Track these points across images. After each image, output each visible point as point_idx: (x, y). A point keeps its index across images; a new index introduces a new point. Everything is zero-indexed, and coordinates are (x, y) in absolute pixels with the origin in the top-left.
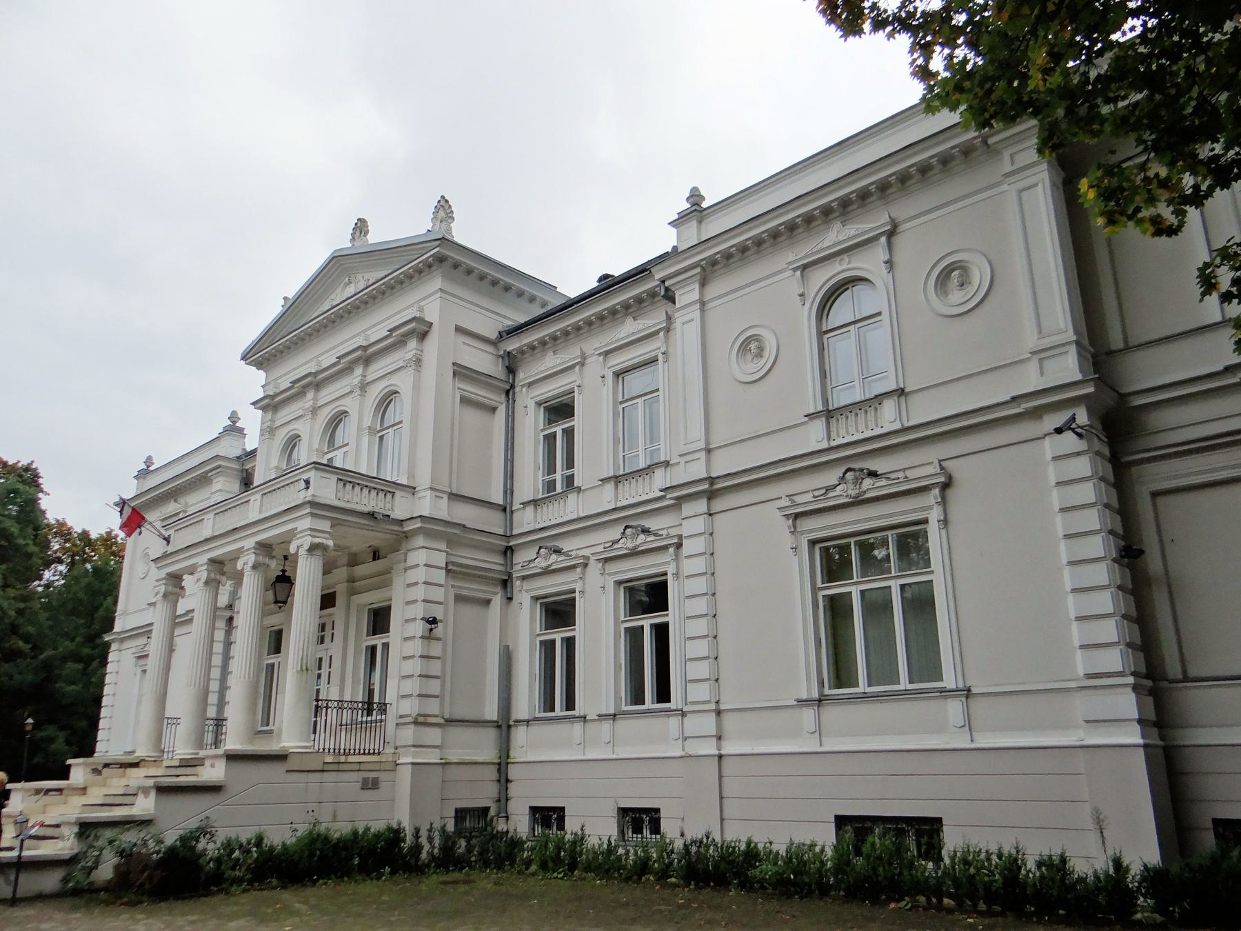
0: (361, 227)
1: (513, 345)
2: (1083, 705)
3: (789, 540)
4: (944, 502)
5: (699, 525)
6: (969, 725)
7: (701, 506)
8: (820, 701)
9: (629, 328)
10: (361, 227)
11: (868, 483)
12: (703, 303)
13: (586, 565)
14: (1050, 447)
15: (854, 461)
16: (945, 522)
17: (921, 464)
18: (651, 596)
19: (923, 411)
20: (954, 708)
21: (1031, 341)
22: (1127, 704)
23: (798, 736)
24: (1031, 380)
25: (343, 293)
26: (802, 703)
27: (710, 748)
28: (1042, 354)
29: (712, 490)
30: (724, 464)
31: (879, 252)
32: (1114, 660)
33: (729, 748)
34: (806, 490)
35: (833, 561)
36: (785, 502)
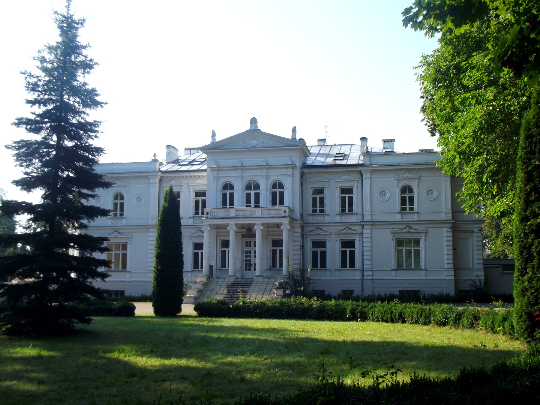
0: (254, 121)
1: (306, 171)
2: (445, 273)
3: (391, 238)
4: (425, 236)
5: (369, 231)
6: (426, 275)
7: (370, 227)
8: (397, 270)
9: (346, 177)
10: (254, 121)
11: (411, 230)
12: (371, 178)
13: (330, 234)
14: (445, 230)
15: (409, 225)
16: (425, 240)
17: (422, 228)
18: (348, 244)
19: (423, 217)
20: (423, 273)
21: (444, 210)
22: (452, 273)
23: (392, 276)
24: (443, 217)
25: (254, 142)
26: (392, 270)
27: (371, 278)
28: (446, 212)
29: (373, 224)
30: (377, 218)
31: (416, 182)
32: (451, 266)
33: (375, 278)
34: (397, 228)
35: (399, 243)
36: (392, 230)
